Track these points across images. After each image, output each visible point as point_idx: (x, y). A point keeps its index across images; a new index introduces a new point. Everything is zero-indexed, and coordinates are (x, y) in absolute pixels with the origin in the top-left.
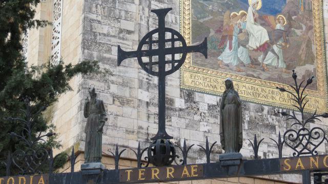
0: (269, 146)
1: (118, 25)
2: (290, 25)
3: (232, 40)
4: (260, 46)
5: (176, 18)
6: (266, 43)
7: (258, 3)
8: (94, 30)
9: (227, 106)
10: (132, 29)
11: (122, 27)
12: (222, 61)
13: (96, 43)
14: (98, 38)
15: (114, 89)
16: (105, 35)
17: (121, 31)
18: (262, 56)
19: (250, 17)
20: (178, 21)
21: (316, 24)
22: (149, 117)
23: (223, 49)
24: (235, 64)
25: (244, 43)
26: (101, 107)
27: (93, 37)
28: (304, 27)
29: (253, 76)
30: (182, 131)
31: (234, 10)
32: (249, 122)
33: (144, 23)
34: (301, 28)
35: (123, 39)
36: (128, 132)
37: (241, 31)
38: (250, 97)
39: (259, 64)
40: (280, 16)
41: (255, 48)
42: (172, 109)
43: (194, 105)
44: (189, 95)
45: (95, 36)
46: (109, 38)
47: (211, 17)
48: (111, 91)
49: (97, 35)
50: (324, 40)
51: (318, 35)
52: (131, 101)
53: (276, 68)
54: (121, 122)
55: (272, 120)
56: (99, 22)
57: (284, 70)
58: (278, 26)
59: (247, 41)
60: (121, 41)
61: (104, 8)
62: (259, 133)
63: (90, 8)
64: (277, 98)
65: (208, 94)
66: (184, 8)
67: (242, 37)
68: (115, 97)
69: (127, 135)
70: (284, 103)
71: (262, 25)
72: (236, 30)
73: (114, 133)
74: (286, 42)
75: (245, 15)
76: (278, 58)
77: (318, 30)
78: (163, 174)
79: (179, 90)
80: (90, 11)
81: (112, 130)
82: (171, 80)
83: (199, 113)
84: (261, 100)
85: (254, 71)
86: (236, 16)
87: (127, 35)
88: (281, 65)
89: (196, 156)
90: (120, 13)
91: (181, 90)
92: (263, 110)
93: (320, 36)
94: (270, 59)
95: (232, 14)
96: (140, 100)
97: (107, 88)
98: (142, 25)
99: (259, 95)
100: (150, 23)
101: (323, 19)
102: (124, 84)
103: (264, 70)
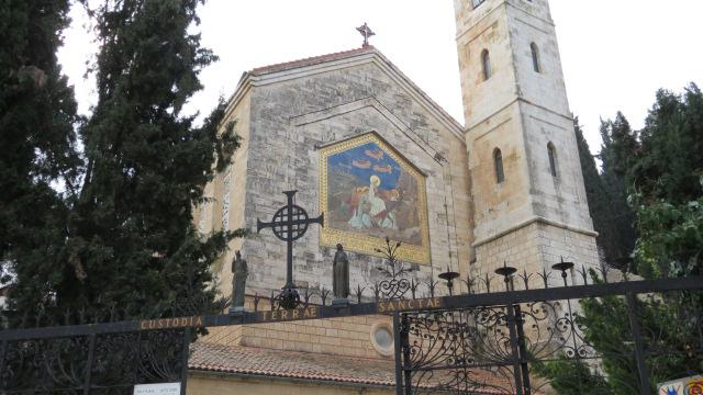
9: (338, 264)
19: (371, 192)
21: (421, 197)
25: (367, 211)
26: (244, 264)
37: (365, 202)
58: (393, 199)
59: (370, 210)
68: (269, 253)
74: (399, 210)
75: (367, 190)
78: (290, 315)
80: (251, 188)
88: (395, 228)
91: (320, 247)
94: (386, 223)
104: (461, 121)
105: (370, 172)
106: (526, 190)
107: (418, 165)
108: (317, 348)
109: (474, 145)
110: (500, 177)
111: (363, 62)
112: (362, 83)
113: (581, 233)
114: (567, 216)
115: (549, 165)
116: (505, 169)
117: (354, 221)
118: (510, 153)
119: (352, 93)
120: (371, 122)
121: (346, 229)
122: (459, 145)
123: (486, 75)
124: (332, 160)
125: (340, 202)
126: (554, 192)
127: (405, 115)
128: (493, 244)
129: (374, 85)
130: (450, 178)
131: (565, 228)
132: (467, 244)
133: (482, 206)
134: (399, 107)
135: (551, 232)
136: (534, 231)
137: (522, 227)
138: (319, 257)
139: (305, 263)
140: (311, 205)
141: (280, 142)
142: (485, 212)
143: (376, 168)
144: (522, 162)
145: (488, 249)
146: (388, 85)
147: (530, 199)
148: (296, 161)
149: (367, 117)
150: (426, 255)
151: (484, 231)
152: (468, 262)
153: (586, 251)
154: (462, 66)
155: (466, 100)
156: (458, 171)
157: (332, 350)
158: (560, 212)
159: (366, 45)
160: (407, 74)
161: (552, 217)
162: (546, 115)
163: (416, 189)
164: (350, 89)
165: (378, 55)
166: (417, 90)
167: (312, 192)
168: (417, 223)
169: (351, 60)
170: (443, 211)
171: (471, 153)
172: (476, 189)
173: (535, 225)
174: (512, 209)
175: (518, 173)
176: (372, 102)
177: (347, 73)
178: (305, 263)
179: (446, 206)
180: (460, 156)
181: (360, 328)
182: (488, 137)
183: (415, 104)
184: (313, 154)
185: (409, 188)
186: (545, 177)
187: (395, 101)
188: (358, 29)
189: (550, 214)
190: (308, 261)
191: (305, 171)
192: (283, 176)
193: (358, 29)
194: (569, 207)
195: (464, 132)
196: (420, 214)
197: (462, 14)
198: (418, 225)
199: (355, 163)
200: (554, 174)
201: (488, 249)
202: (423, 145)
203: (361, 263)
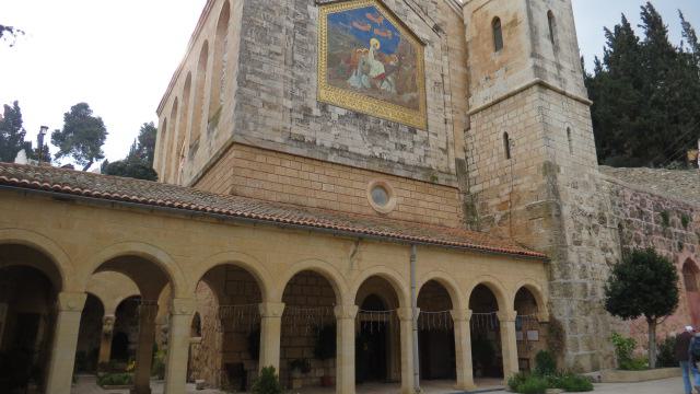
2: (400, 63)
10: (280, 52)
15: (263, 96)
17: (271, 53)
21: (419, 64)
24: (360, 86)
25: (367, 73)
30: (318, 133)
32: (370, 130)
33: (289, 48)
34: (408, 66)
36: (274, 130)
40: (393, 56)
44: (324, 107)
54: (269, 122)
58: (392, 63)
67: (365, 68)
68: (264, 103)
73: (264, 129)
74: (397, 74)
80: (246, 34)
84: (379, 115)
88: (394, 91)
94: (385, 86)
102: (273, 93)
105: (370, 35)
107: (416, 33)
108: (313, 202)
109: (472, 17)
110: (498, 44)
113: (577, 100)
116: (505, 35)
117: (353, 80)
118: (510, 19)
121: (345, 87)
122: (457, 20)
124: (332, 18)
125: (339, 62)
126: (553, 59)
128: (489, 110)
130: (447, 49)
131: (564, 93)
132: (462, 113)
133: (478, 75)
135: (551, 97)
136: (535, 94)
137: (522, 90)
138: (316, 112)
139: (301, 117)
140: (310, 59)
142: (482, 80)
143: (376, 31)
144: (524, 27)
147: (531, 62)
148: (295, 15)
151: (479, 99)
153: (581, 118)
156: (455, 43)
157: (329, 205)
158: (559, 78)
161: (552, 82)
163: (415, 55)
167: (311, 47)
168: (415, 89)
170: (440, 79)
171: (469, 27)
172: (473, 60)
173: (535, 88)
174: (511, 74)
175: (519, 40)
178: (301, 117)
179: (442, 75)
180: (457, 30)
181: (356, 185)
182: (485, 8)
186: (545, 42)
189: (549, 79)
191: (304, 25)
192: (280, 27)
194: (565, 74)
196: (418, 81)
198: (416, 91)
200: (553, 42)
202: (422, 14)
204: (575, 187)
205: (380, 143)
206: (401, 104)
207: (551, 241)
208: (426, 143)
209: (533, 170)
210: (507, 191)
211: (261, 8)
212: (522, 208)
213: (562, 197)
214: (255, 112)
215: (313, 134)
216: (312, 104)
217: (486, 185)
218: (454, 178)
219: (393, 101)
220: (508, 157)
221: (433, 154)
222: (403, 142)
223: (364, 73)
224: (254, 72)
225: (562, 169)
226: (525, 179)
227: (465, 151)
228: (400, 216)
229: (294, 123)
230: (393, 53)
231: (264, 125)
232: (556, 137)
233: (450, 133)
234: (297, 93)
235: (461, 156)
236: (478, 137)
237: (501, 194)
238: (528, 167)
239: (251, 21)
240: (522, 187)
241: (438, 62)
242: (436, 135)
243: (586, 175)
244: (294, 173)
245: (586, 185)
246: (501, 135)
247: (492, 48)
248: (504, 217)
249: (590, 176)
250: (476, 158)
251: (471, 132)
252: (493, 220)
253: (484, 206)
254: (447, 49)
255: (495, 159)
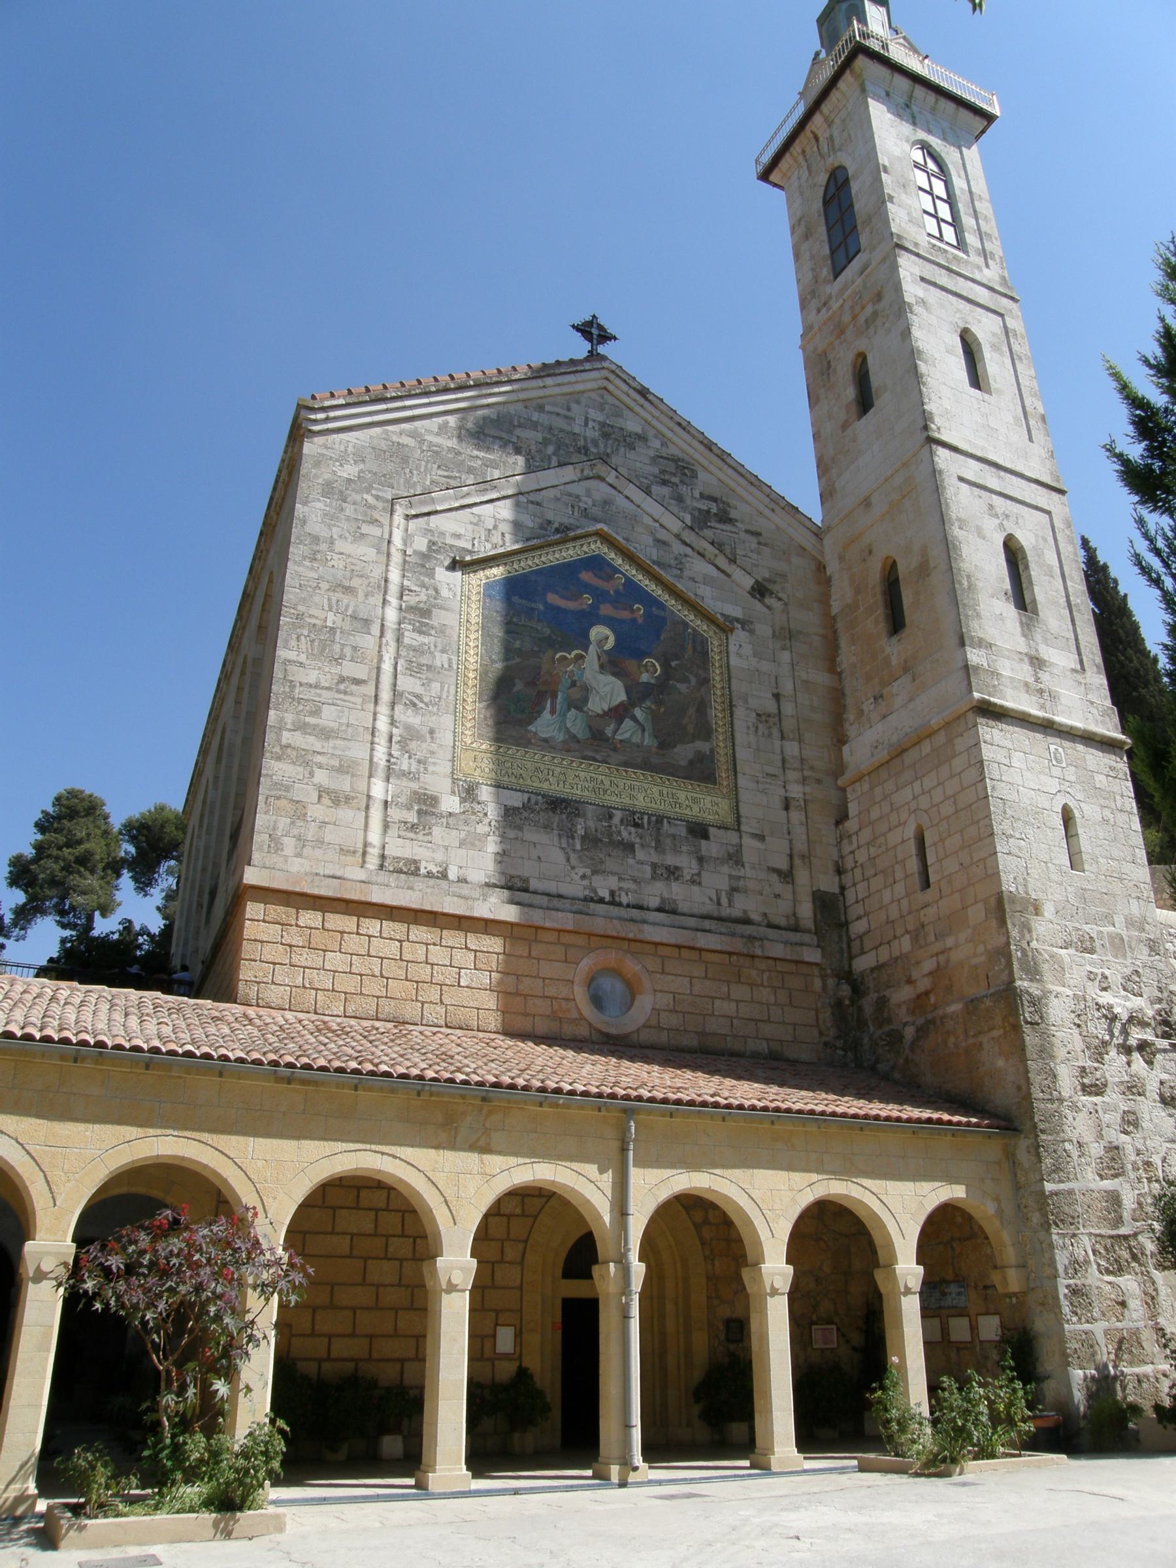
0: (620, 879)
1: (336, 670)
3: (556, 697)
4: (610, 710)
5: (450, 660)
6: (621, 704)
7: (607, 638)
8: (290, 678)
11: (345, 674)
12: (535, 733)
13: (293, 699)
14: (297, 691)
15: (321, 777)
16: (311, 686)
17: (342, 680)
18: (612, 726)
20: (455, 667)
21: (716, 675)
22: (386, 826)
23: (540, 713)
24: (561, 738)
25: (578, 704)
27: (287, 690)
28: (693, 680)
29: (595, 760)
31: (562, 649)
32: (584, 838)
33: (387, 667)
34: (685, 680)
35: (345, 693)
36: (343, 851)
37: (574, 684)
38: (587, 795)
39: (607, 740)
41: (600, 712)
42: (434, 814)
43: (477, 807)
45: (293, 687)
46: (318, 691)
47: (518, 660)
48: (316, 780)
49: (295, 686)
50: (731, 702)
51: (719, 693)
52: (353, 798)
53: (638, 746)
54: (330, 835)
55: (628, 834)
56: (301, 664)
57: (654, 750)
58: (645, 677)
59: (585, 700)
60: (342, 696)
61: (312, 641)
62: (601, 856)
63: (287, 641)
64: (640, 797)
65: (507, 788)
66: (467, 644)
67: (575, 694)
68: (322, 792)
69: (343, 858)
70: (653, 805)
71: (615, 674)
72: (566, 681)
73: (318, 853)
74: (660, 703)
75: (580, 658)
76: (643, 730)
77: (719, 686)
79: (450, 780)
81: (313, 848)
82: (434, 764)
83: (486, 821)
85: (596, 751)
86: (566, 658)
87: (354, 687)
89: (476, 894)
90: (342, 650)
92: (611, 817)
93: (723, 695)
94: (627, 731)
95: (557, 656)
96: (369, 797)
97: (307, 775)
98: (382, 671)
99: (605, 791)
100: (399, 668)
101: (728, 666)
102: (344, 768)
103: (615, 750)
104: (813, 510)
105: (590, 617)
106: (953, 641)
109: (841, 559)
110: (896, 622)
111: (580, 387)
112: (577, 430)
114: (1053, 696)
115: (1007, 585)
117: (545, 725)
119: (550, 449)
120: (596, 511)
123: (864, 402)
126: (1021, 645)
127: (680, 499)
129: (606, 436)
130: (787, 636)
134: (665, 483)
137: (947, 725)
138: (450, 803)
139: (412, 817)
140: (436, 686)
141: (367, 552)
142: (868, 706)
143: (606, 610)
145: (872, 788)
146: (642, 438)
149: (586, 502)
150: (724, 806)
152: (833, 821)
153: (1101, 780)
154: (814, 399)
155: (824, 467)
156: (808, 620)
159: (593, 356)
160: (685, 413)
162: (999, 477)
163: (704, 655)
164: (545, 442)
165: (618, 372)
166: (709, 446)
167: (440, 660)
168: (705, 732)
169: (549, 381)
170: (770, 706)
172: (848, 656)
176: (601, 469)
177: (541, 409)
178: (412, 817)
179: (777, 696)
181: (547, 969)
183: (702, 475)
184: (449, 581)
185: (689, 653)
187: (656, 471)
188: (576, 328)
189: (1009, 692)
190: (419, 812)
191: (426, 613)
192: (367, 622)
193: (576, 328)
195: (818, 533)
196: (716, 713)
197: (813, 293)
199: (553, 599)
201: (872, 788)
202: (722, 561)
203: (556, 819)
204: (1092, 951)
205: (610, 864)
206: (669, 770)
207: (1019, 1088)
208: (735, 857)
209: (976, 914)
210: (928, 965)
211: (325, 586)
212: (955, 1007)
213: (1048, 976)
214: (299, 813)
215: (439, 856)
216: (439, 782)
217: (884, 955)
218: (807, 938)
219: (646, 766)
220: (926, 884)
221: (751, 885)
222: (670, 860)
223: (573, 704)
224: (301, 727)
225: (1048, 910)
226: (962, 936)
227: (840, 871)
228: (664, 1038)
229: (393, 832)
230: (649, 655)
231: (320, 842)
232: (1029, 830)
233: (799, 832)
234: (405, 764)
235: (829, 884)
236: (865, 836)
237: (915, 974)
238: (965, 908)
239: (300, 616)
240: (955, 957)
241: (765, 666)
242: (761, 838)
243: (1119, 920)
244: (392, 948)
245: (1119, 945)
246: (910, 831)
247: (882, 627)
248: (922, 1032)
249: (1130, 923)
250: (861, 888)
251: (851, 825)
252: (902, 1037)
253: (882, 1003)
254: (787, 636)
255: (900, 889)
